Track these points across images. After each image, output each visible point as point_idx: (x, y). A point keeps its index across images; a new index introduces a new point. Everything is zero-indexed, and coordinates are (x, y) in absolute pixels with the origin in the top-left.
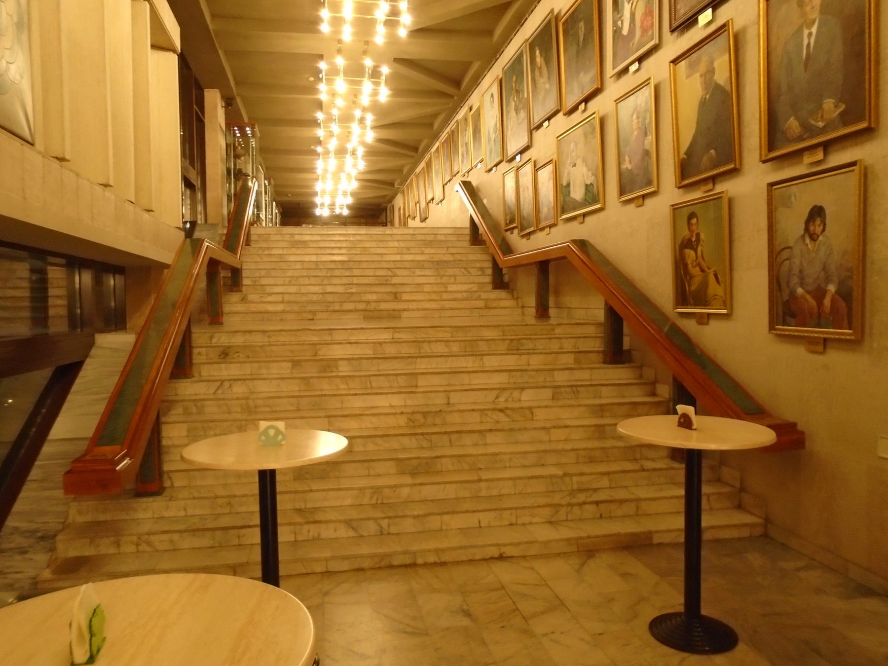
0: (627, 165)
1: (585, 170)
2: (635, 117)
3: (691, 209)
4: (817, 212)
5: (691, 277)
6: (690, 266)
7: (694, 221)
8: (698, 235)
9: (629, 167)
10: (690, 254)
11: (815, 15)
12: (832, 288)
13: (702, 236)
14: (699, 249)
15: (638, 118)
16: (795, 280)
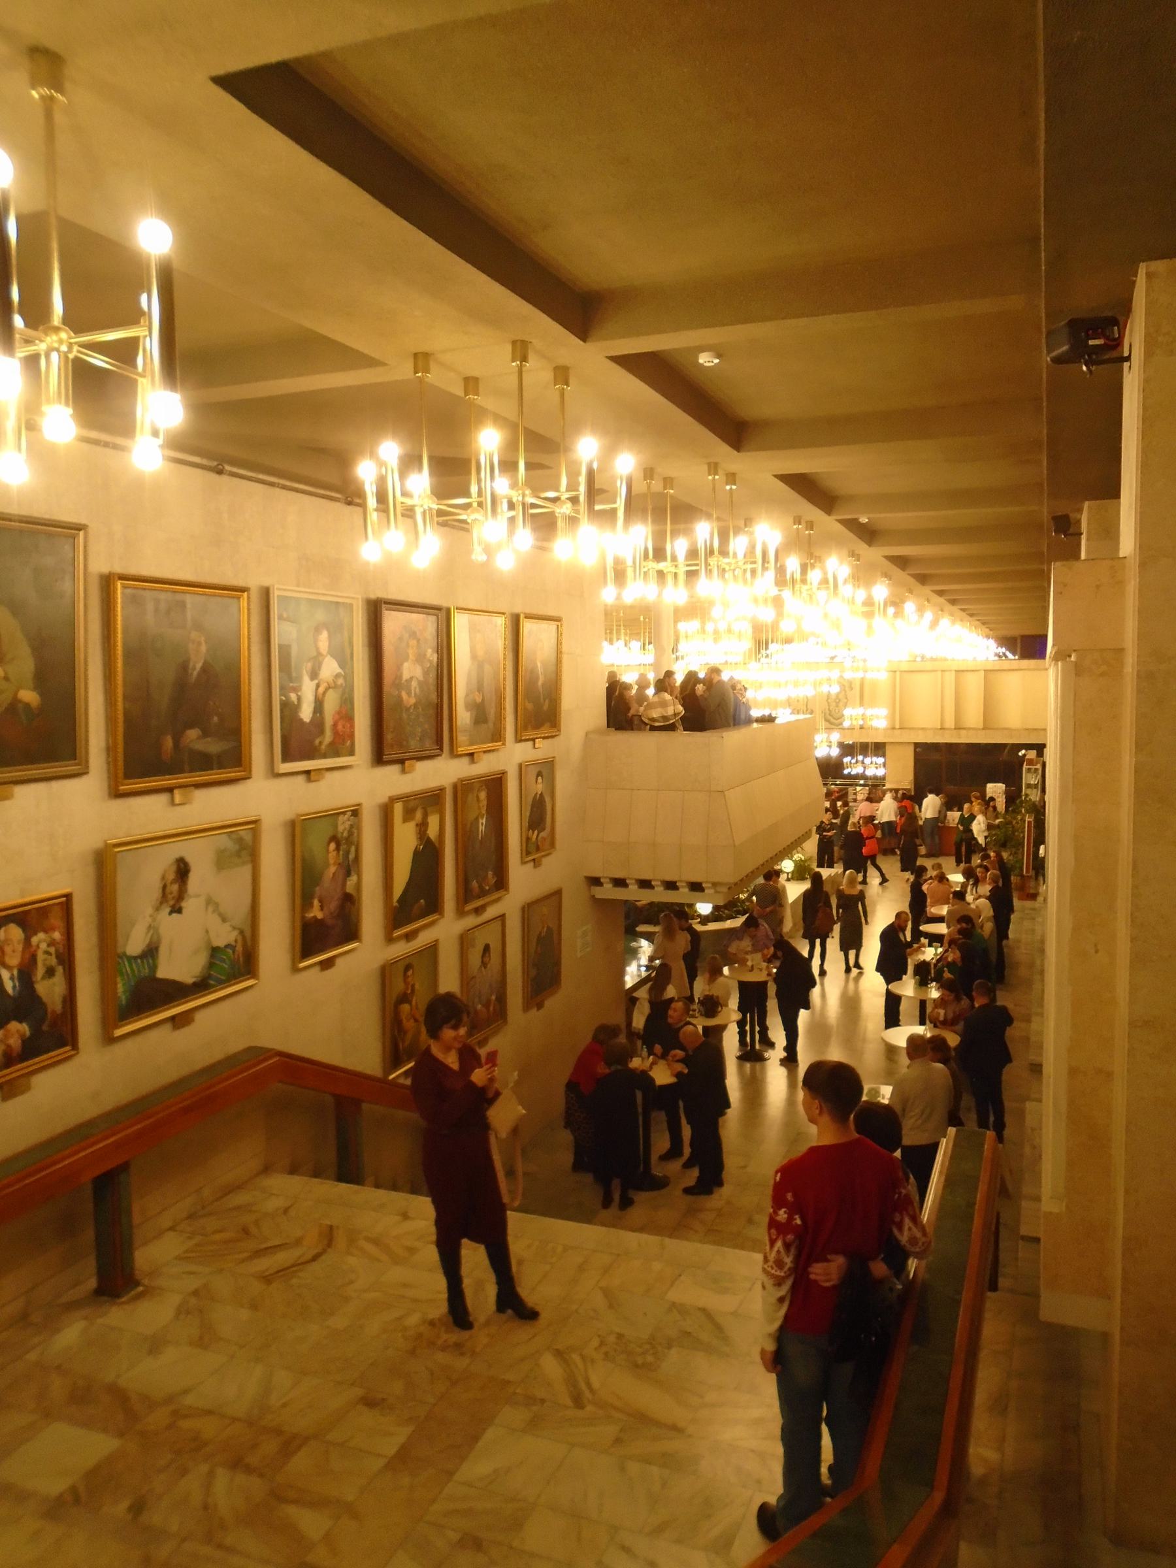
0: (316, 912)
1: (213, 921)
2: (333, 846)
3: (407, 961)
4: (487, 948)
5: (405, 1033)
6: (404, 1021)
7: (410, 973)
8: (413, 986)
9: (320, 915)
10: (405, 1008)
11: (484, 812)
12: (493, 997)
13: (417, 987)
14: (414, 1003)
15: (338, 849)
16: (477, 1000)
